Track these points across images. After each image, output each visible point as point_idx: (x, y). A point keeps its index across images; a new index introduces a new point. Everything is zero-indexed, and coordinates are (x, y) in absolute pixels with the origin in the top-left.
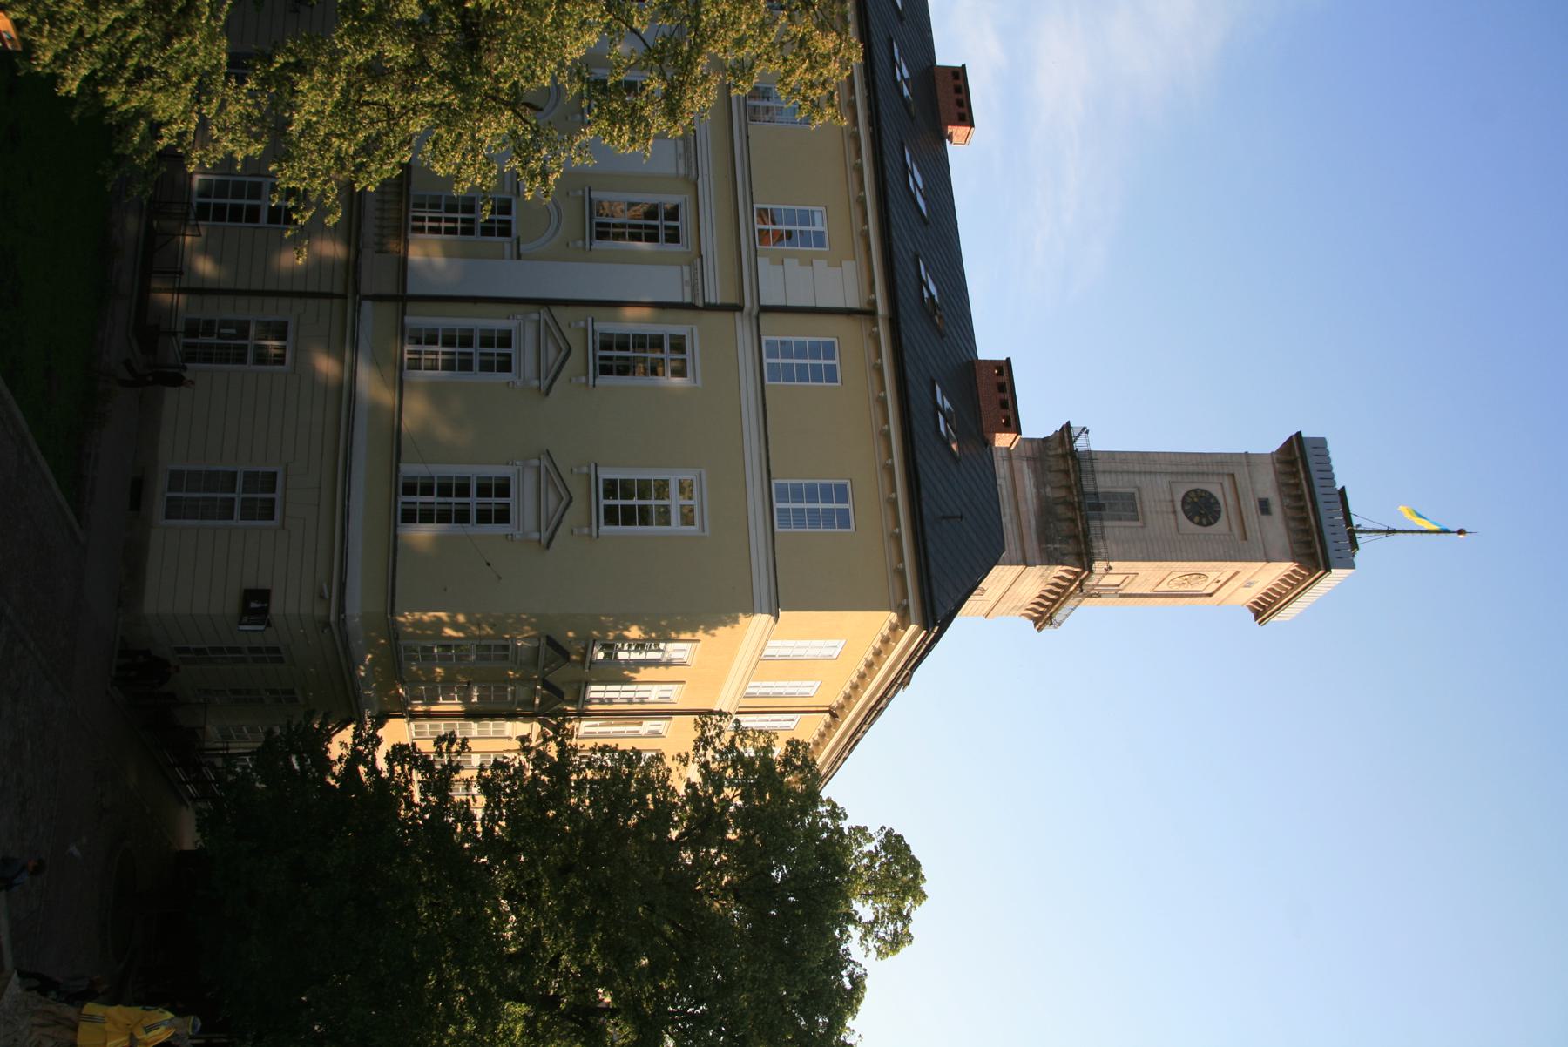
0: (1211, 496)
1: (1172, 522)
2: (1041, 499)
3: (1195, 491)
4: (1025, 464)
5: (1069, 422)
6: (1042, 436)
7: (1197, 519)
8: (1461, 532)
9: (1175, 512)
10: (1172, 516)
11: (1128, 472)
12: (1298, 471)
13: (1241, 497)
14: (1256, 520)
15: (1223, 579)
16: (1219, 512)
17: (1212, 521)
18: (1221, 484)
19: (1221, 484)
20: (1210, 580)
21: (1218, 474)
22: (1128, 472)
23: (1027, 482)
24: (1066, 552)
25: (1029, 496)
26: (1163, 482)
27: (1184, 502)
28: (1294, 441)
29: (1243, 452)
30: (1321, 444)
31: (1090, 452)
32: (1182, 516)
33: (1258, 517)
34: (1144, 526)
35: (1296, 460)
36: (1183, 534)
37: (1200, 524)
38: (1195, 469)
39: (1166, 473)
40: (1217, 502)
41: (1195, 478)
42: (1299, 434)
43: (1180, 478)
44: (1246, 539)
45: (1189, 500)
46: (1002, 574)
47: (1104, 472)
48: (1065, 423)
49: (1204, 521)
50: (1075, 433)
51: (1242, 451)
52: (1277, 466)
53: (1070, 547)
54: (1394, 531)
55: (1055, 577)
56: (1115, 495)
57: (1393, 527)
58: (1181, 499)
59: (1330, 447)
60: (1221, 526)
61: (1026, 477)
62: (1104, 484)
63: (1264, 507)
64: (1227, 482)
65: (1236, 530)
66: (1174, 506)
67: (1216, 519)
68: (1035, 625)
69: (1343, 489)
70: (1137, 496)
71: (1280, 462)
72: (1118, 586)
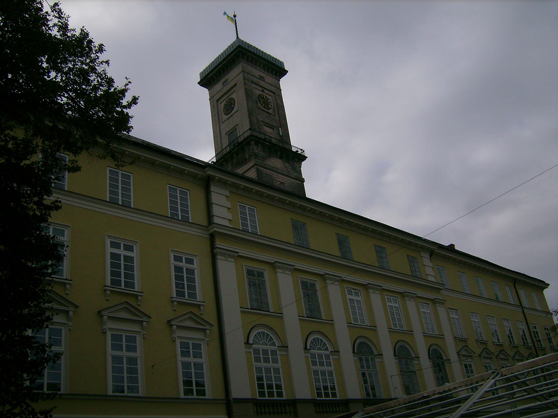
9: (232, 116)
10: (233, 116)
11: (221, 141)
16: (229, 99)
17: (233, 100)
18: (221, 103)
19: (221, 103)
22: (221, 141)
26: (223, 126)
28: (201, 84)
30: (201, 74)
34: (237, 125)
36: (238, 108)
42: (199, 83)
44: (236, 84)
60: (234, 96)
66: (230, 117)
70: (228, 133)
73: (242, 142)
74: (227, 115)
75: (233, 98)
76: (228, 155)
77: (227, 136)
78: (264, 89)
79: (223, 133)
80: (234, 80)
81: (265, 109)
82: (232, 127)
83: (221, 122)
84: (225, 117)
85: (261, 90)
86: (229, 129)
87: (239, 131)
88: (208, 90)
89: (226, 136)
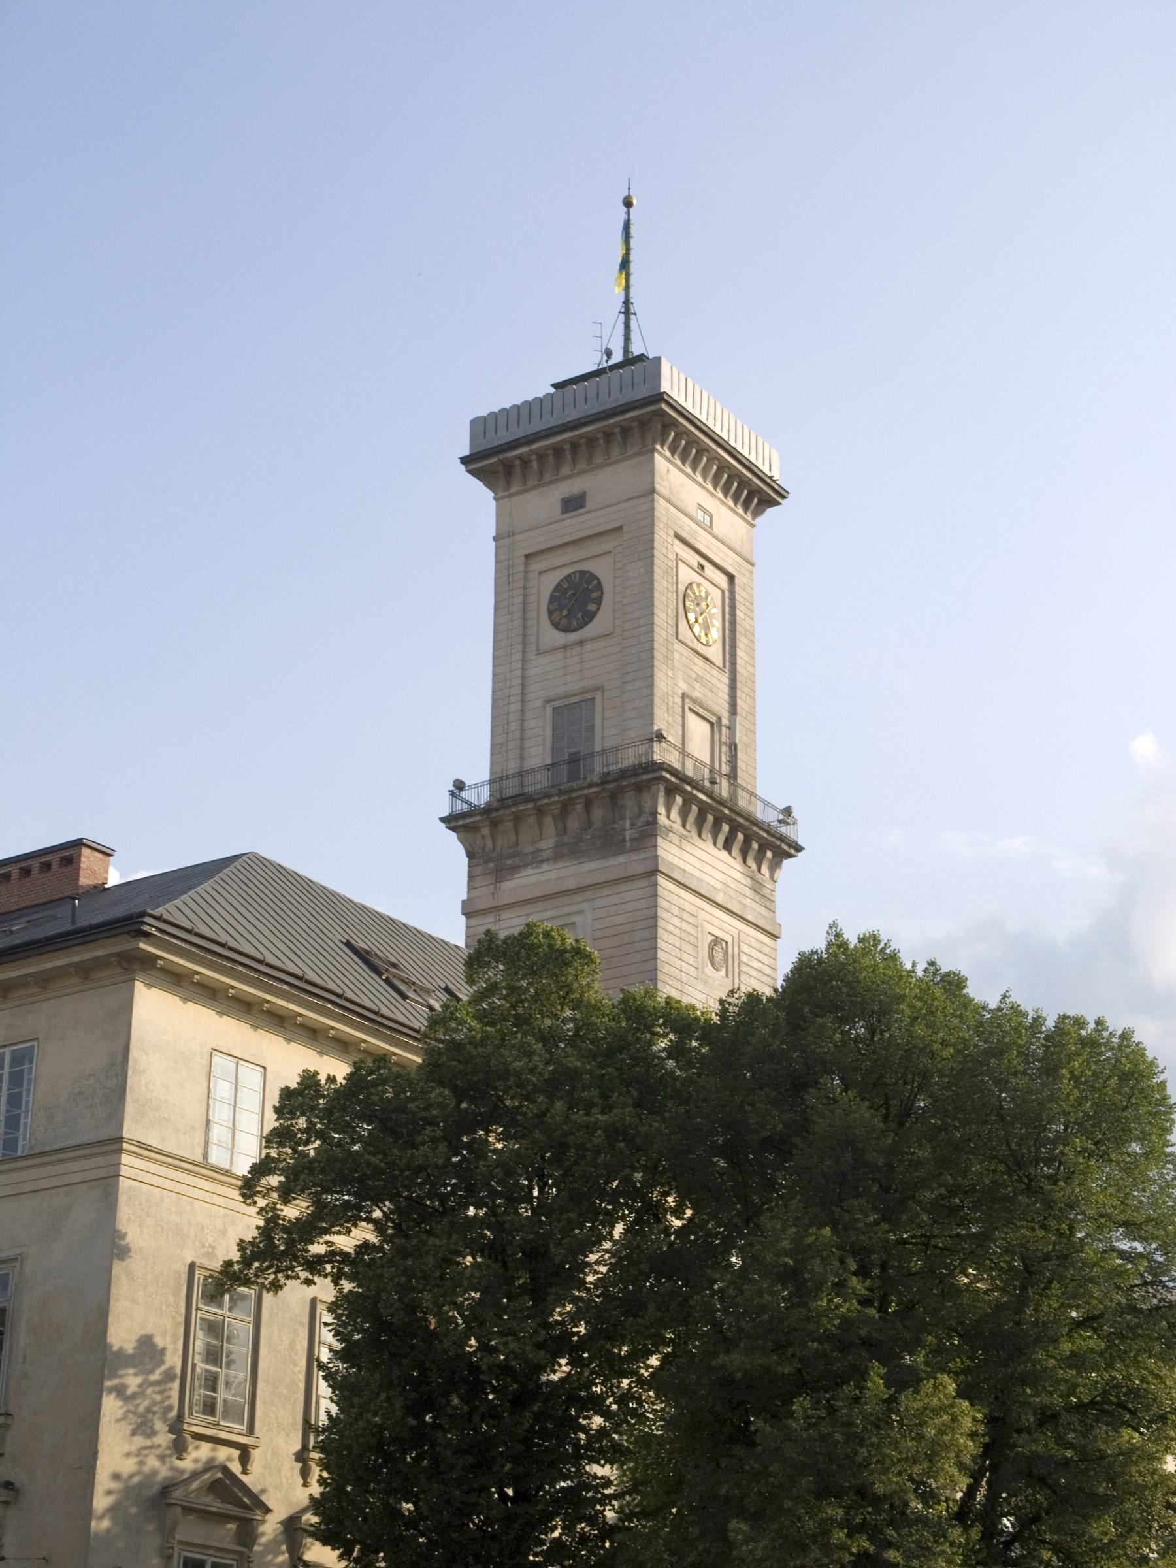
0: (558, 588)
1: (598, 644)
2: (560, 854)
3: (550, 613)
4: (506, 885)
5: (443, 820)
6: (464, 861)
7: (592, 607)
8: (628, 203)
9: (581, 643)
10: (588, 647)
12: (520, 457)
13: (559, 541)
14: (593, 515)
15: (694, 559)
16: (582, 573)
17: (595, 582)
18: (540, 573)
19: (540, 573)
20: (696, 578)
21: (526, 579)
23: (533, 879)
24: (636, 809)
25: (553, 875)
26: (538, 666)
27: (567, 630)
29: (493, 544)
30: (480, 426)
31: (492, 782)
32: (589, 630)
33: (589, 512)
34: (599, 688)
35: (502, 462)
36: (614, 628)
37: (599, 601)
38: (518, 615)
39: (524, 661)
40: (568, 578)
41: (532, 614)
42: (465, 461)
43: (532, 639)
45: (564, 621)
46: (675, 910)
47: (522, 758)
48: (443, 825)
49: (594, 595)
50: (460, 807)
51: (492, 545)
52: (513, 490)
53: (629, 801)
54: (627, 303)
55: (684, 826)
56: (556, 738)
57: (619, 306)
58: (563, 635)
59: (484, 412)
60: (602, 569)
61: (524, 881)
62: (539, 755)
63: (574, 504)
64: (538, 565)
65: (606, 544)
67: (592, 577)
68: (790, 856)
69: (554, 386)
71: (508, 485)
72: (712, 724)
73: (624, 774)
74: (561, 630)
75: (598, 579)
76: (556, 799)
77: (549, 710)
78: (704, 562)
79: (537, 694)
80: (614, 509)
81: (700, 645)
82: (576, 687)
83: (532, 648)
84: (553, 637)
85: (695, 565)
86: (561, 691)
87: (603, 715)
88: (495, 499)
89: (544, 708)
